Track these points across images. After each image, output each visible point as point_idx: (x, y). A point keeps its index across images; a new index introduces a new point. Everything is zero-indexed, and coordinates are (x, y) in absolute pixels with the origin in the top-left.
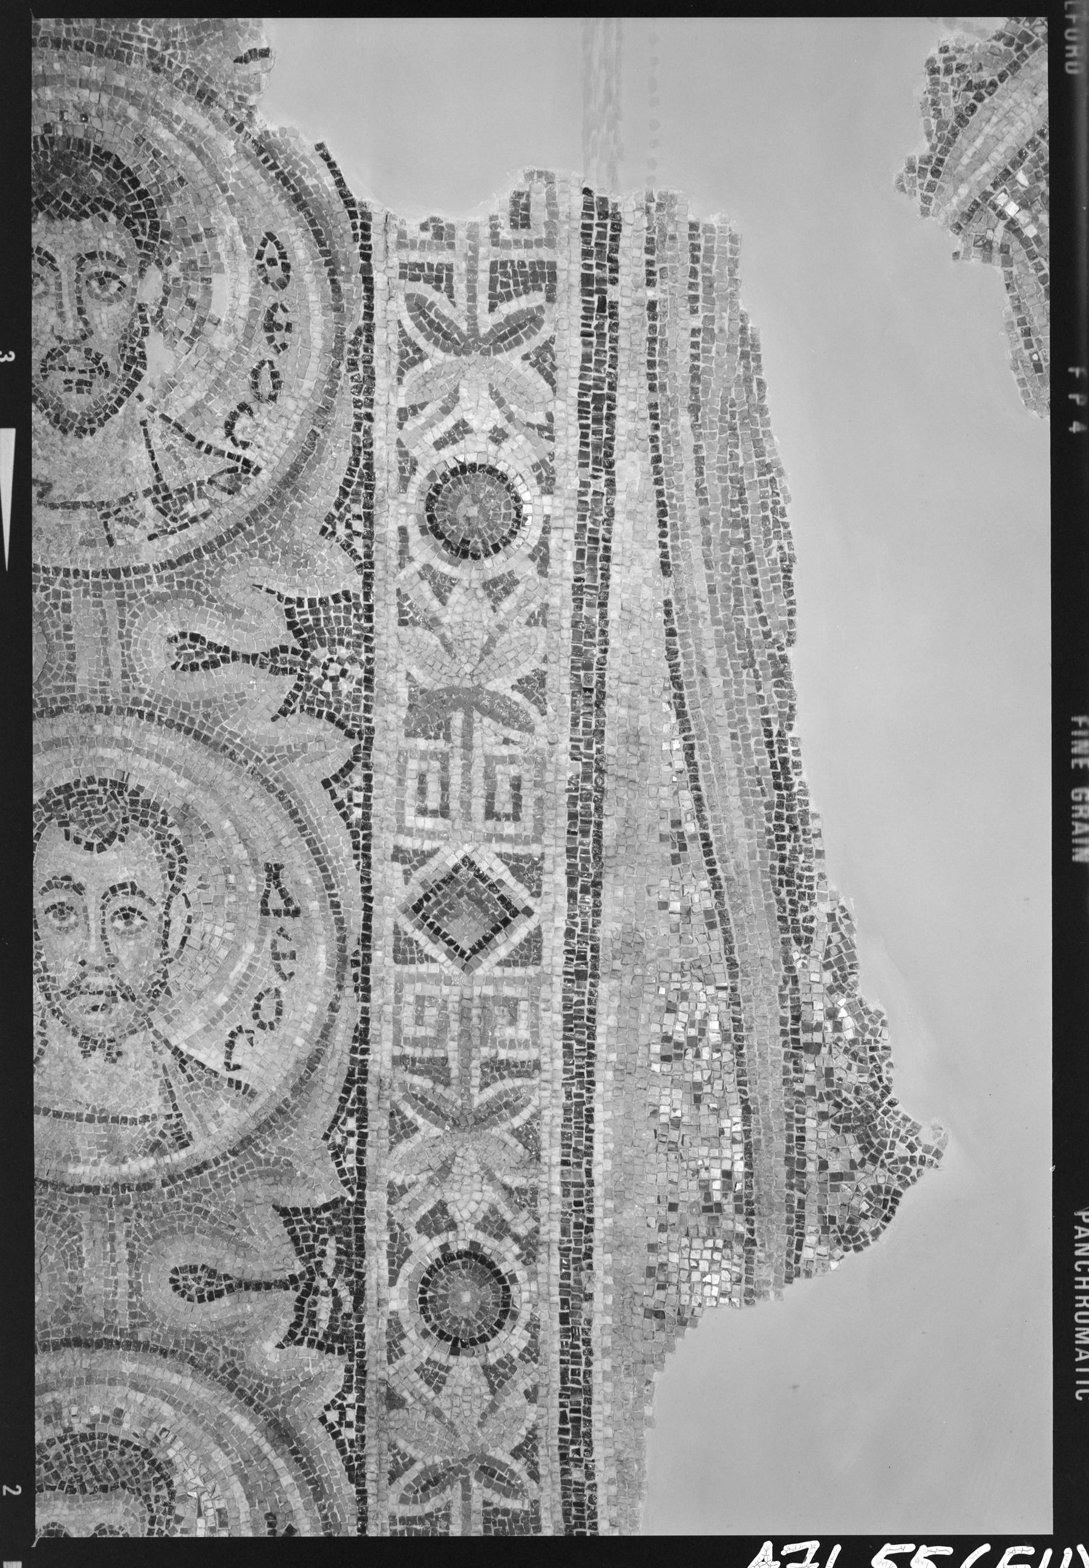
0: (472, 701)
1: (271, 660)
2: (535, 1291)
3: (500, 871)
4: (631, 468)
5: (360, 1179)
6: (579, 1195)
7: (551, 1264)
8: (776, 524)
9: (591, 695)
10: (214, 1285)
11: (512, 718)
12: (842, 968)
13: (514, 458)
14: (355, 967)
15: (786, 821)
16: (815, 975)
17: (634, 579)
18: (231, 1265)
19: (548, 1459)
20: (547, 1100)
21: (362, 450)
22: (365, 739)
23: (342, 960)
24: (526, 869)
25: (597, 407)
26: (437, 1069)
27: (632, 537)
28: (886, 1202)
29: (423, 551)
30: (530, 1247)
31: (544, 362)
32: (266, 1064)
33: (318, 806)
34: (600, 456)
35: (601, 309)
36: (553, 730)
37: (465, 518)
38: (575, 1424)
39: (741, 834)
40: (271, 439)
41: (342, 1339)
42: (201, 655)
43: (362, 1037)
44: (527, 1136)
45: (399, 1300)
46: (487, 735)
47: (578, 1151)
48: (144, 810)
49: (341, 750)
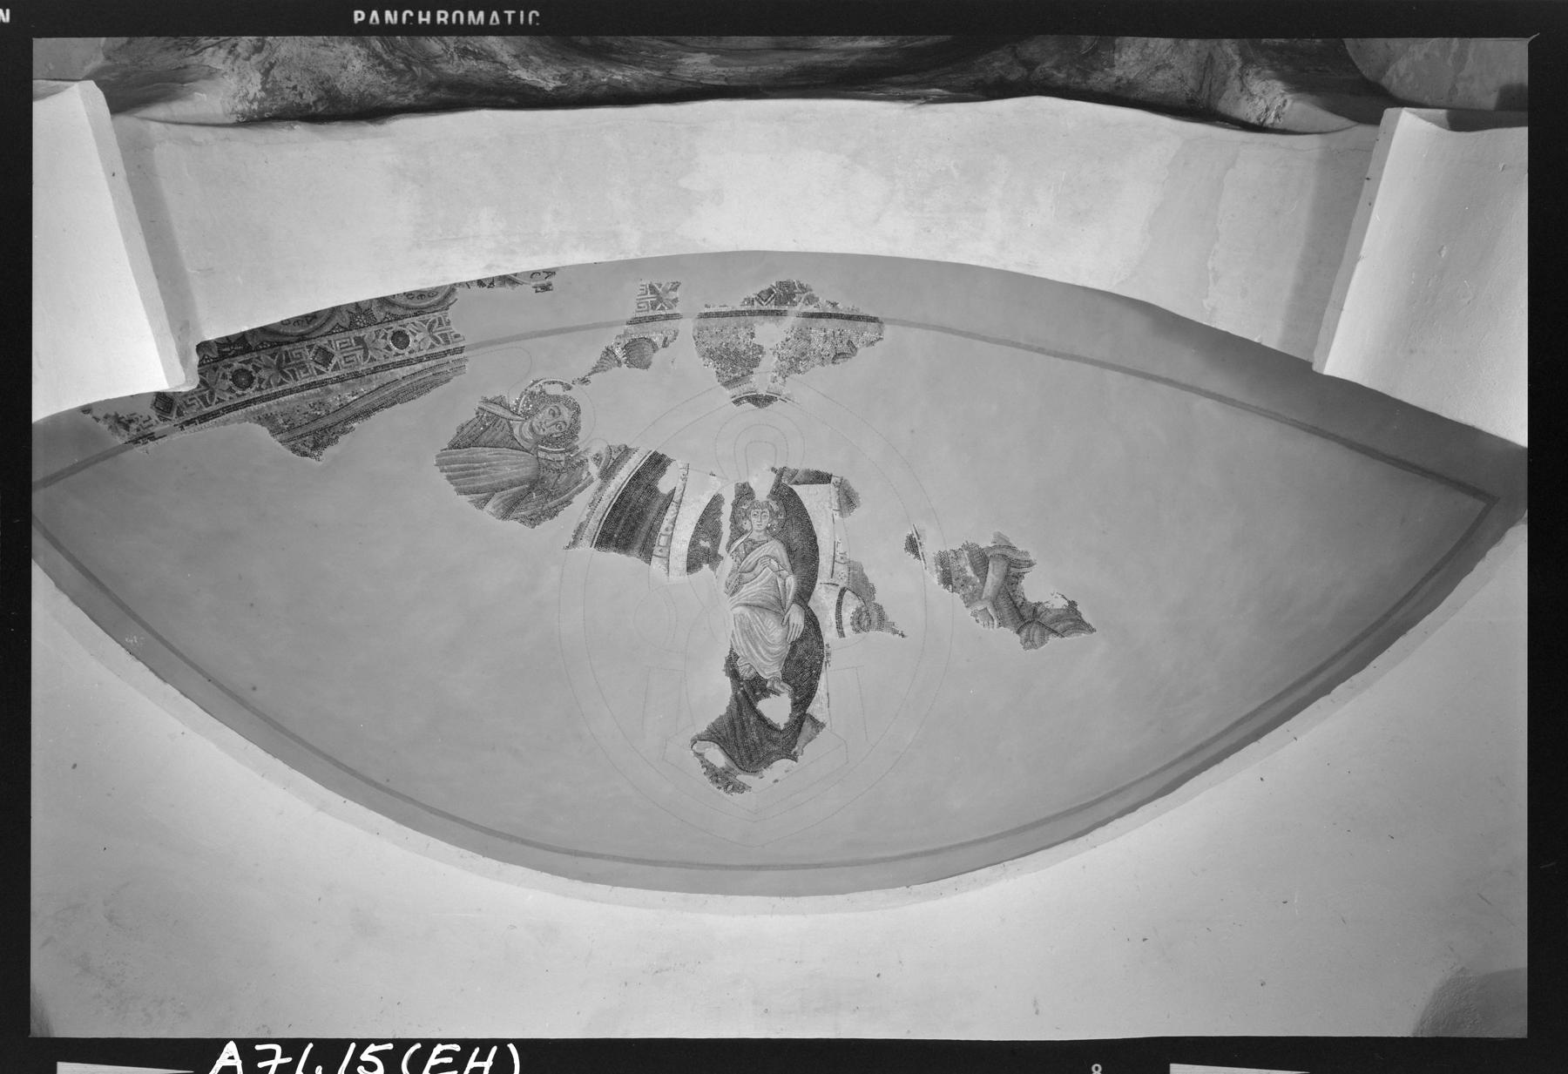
0: (366, 349)
2: (251, 393)
3: (334, 362)
4: (419, 367)
5: (257, 350)
6: (276, 396)
7: (258, 395)
8: (420, 394)
9: (375, 371)
11: (365, 357)
12: (344, 432)
16: (339, 428)
17: (400, 372)
19: (221, 405)
20: (290, 385)
21: (405, 317)
23: (302, 335)
24: (336, 367)
25: (429, 357)
26: (288, 360)
27: (407, 371)
28: (305, 454)
29: (390, 333)
30: (260, 389)
31: (432, 346)
33: (333, 323)
34: (420, 360)
35: (445, 353)
37: (400, 338)
38: (229, 409)
43: (288, 343)
44: (282, 383)
45: (236, 365)
46: (360, 353)
47: (284, 393)
49: (345, 325)
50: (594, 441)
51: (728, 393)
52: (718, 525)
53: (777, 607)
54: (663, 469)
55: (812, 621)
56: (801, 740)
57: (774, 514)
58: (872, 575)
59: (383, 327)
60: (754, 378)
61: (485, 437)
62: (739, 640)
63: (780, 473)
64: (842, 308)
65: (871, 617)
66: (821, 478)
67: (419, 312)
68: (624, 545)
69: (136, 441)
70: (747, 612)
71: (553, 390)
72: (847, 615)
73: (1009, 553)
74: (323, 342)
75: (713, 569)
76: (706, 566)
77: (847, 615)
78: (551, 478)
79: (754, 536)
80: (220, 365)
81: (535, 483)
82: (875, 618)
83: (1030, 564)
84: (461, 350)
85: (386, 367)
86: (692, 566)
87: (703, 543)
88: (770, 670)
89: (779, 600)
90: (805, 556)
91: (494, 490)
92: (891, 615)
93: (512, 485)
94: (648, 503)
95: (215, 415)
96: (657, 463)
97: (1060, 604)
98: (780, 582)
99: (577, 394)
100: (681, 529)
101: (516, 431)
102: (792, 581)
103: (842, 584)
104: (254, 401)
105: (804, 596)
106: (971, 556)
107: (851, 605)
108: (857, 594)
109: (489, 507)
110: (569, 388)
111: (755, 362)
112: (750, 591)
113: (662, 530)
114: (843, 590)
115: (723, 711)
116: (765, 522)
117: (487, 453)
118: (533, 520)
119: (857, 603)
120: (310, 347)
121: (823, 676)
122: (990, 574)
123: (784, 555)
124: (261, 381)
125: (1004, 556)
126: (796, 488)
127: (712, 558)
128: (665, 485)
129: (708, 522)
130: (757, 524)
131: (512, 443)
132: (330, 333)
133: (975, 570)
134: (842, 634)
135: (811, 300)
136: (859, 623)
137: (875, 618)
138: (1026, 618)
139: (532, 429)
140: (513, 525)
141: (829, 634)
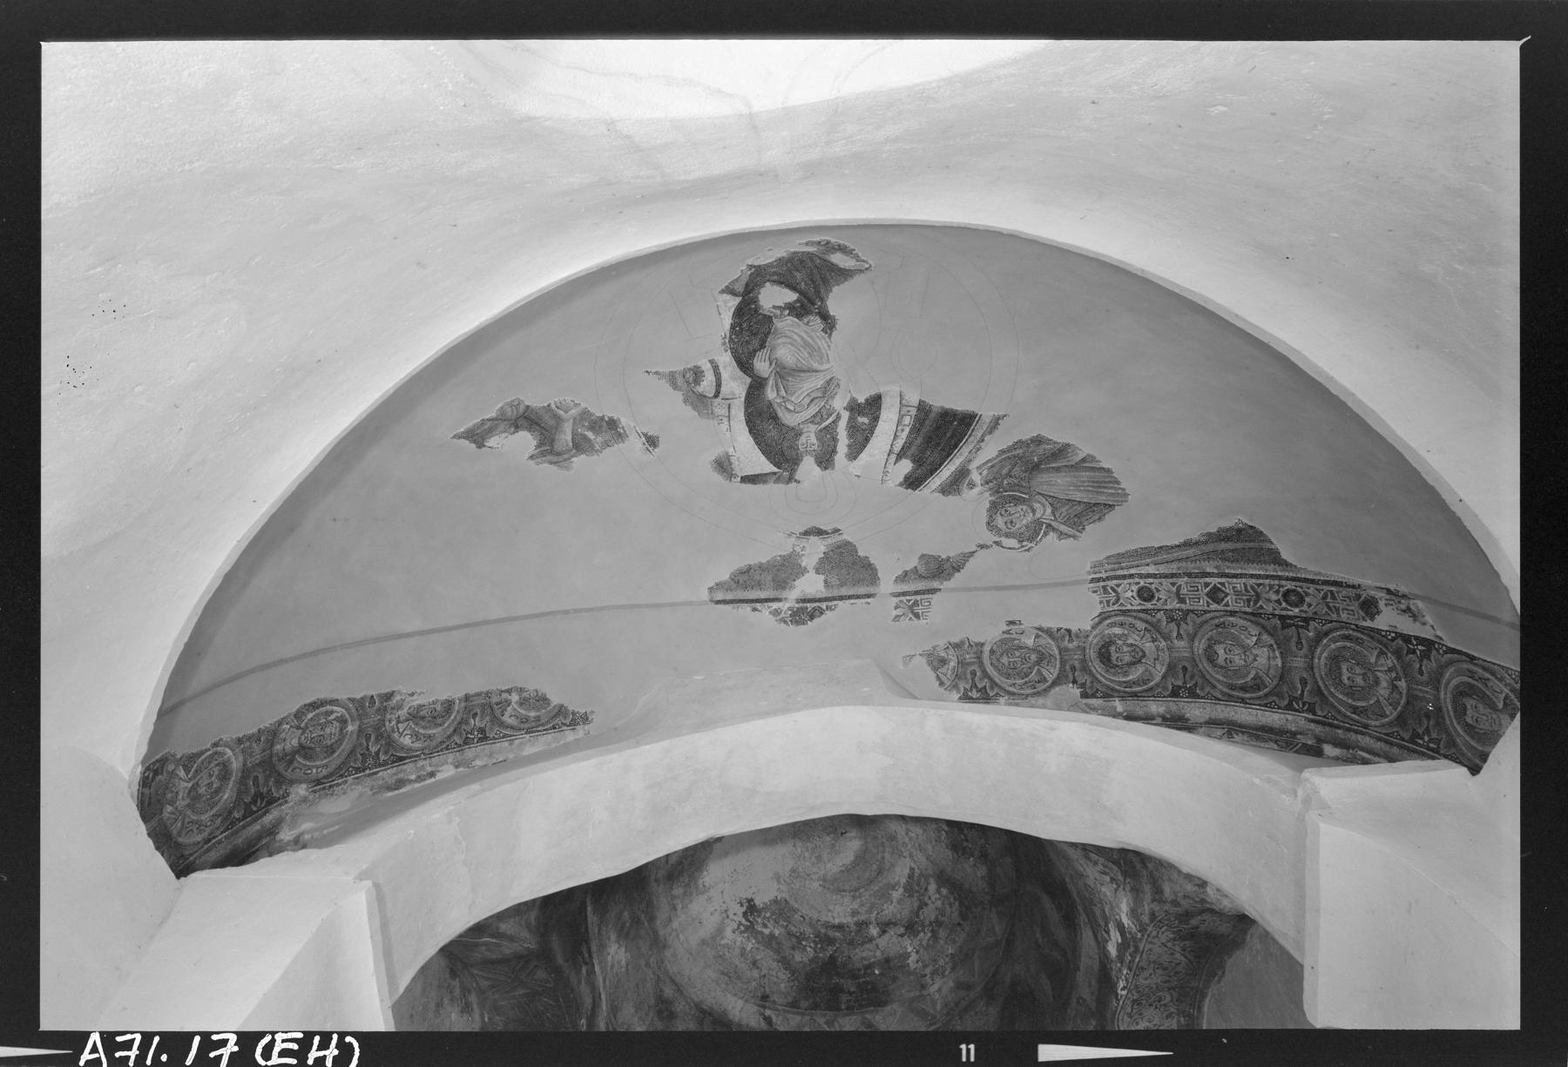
1: (1179, 626)
2: (1289, 585)
4: (1133, 571)
5: (1274, 615)
6: (1267, 577)
9: (1173, 576)
10: (1299, 643)
13: (1135, 588)
14: (1233, 613)
15: (1187, 544)
17: (1151, 570)
18: (1295, 639)
22: (1189, 611)
24: (1207, 585)
25: (1124, 577)
27: (1144, 570)
32: (1254, 630)
34: (1131, 576)
36: (1182, 581)
37: (1146, 594)
38: (1313, 581)
39: (1190, 552)
40: (1140, 625)
41: (1306, 620)
42: (1179, 636)
48: (1210, 647)
50: (976, 499)
51: (846, 537)
52: (850, 436)
53: (783, 373)
54: (907, 478)
55: (744, 365)
56: (745, 279)
57: (794, 447)
58: (689, 412)
59: (1159, 605)
60: (823, 549)
61: (1079, 508)
62: (822, 344)
63: (790, 479)
64: (747, 608)
66: (748, 479)
67: (1125, 613)
68: (947, 416)
69: (1404, 596)
70: (815, 365)
71: (1013, 542)
72: (709, 378)
73: (555, 459)
74: (1214, 606)
75: (853, 400)
76: (861, 400)
78: (1017, 471)
79: (813, 428)
80: (1310, 614)
81: (1035, 468)
82: (680, 381)
83: (532, 457)
84: (1092, 581)
85: (1166, 576)
86: (875, 403)
88: (786, 324)
89: (782, 377)
90: (760, 416)
91: (1076, 467)
92: (664, 385)
93: (1058, 469)
94: (923, 451)
95: (1326, 583)
96: (913, 482)
97: (492, 442)
98: (783, 393)
99: (989, 538)
100: (889, 430)
101: (1049, 510)
102: (770, 394)
103: (718, 400)
104: (1287, 579)
105: (756, 387)
106: (592, 447)
108: (702, 397)
109: (1081, 456)
110: (996, 543)
111: (822, 562)
112: (814, 383)
113: (907, 430)
114: (717, 395)
115: (836, 289)
117: (1078, 496)
118: (1038, 441)
119: (700, 389)
120: (1227, 605)
121: (728, 327)
122: (569, 438)
123: (780, 414)
124: (1277, 592)
125: (558, 454)
127: (854, 408)
128: (906, 466)
129: (860, 439)
131: (1055, 503)
132: (1206, 612)
133: (585, 438)
134: (711, 362)
135: (776, 613)
136: (697, 374)
137: (680, 381)
138: (526, 419)
139: (1034, 511)
140: (1060, 438)
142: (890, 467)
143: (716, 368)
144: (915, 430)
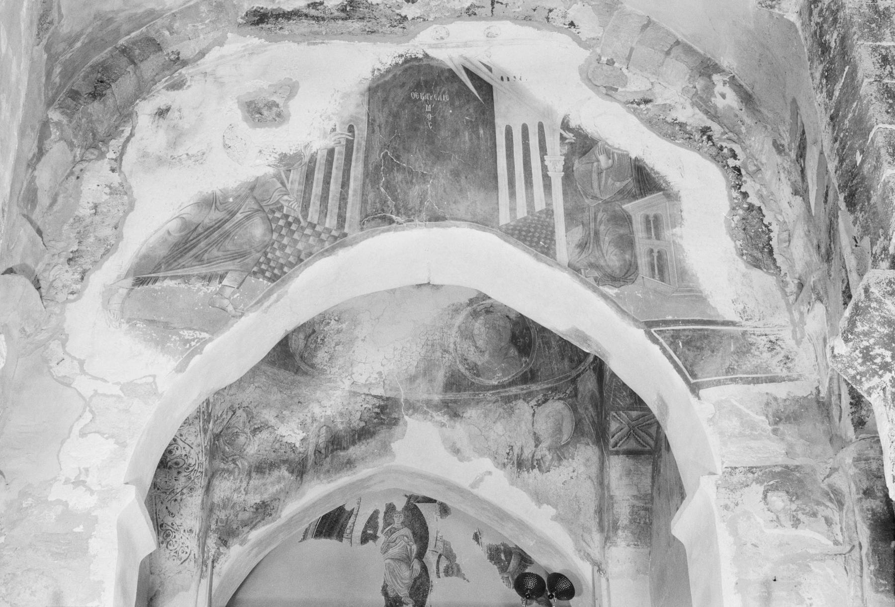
52: (377, 523)
53: (406, 560)
55: (424, 568)
57: (406, 517)
62: (388, 577)
63: (410, 498)
65: (453, 570)
68: (329, 535)
70: (391, 562)
72: (442, 568)
77: (442, 568)
79: (395, 526)
82: (455, 570)
86: (365, 539)
87: (369, 532)
90: (422, 536)
100: (358, 525)
102: (415, 548)
103: (440, 552)
105: (421, 555)
107: (444, 563)
114: (440, 556)
116: (402, 520)
122: (512, 561)
123: (411, 535)
126: (417, 504)
127: (375, 537)
129: (372, 521)
130: (398, 520)
137: (455, 570)
141: (433, 576)
142: (356, 506)
143: (438, 573)
144: (343, 527)
